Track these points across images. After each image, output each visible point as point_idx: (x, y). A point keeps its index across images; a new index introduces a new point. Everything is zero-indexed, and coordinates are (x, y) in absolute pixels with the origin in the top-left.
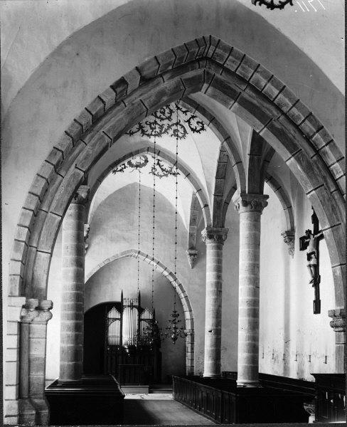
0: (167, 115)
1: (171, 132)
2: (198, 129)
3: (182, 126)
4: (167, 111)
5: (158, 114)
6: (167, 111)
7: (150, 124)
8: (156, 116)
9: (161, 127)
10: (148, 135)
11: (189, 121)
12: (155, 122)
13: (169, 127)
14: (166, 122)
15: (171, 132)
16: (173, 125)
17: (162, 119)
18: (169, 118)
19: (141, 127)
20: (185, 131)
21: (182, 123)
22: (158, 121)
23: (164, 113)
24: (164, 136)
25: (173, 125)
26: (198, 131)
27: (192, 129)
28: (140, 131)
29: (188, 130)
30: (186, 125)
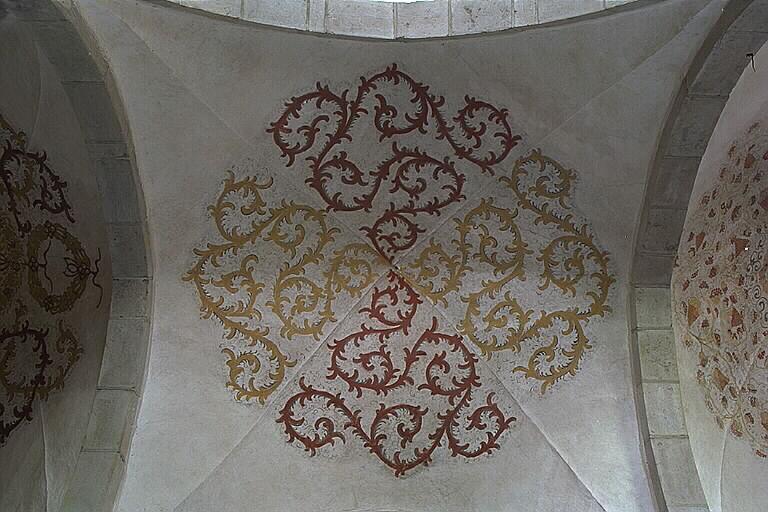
0: (298, 320)
1: (239, 346)
2: (299, 429)
3: (280, 377)
4: (312, 317)
5: (292, 293)
6: (312, 317)
7: (246, 274)
8: (278, 290)
9: (248, 312)
10: (195, 274)
11: (309, 392)
12: (254, 292)
13: (258, 336)
14: (271, 319)
15: (239, 346)
16: (270, 345)
17: (277, 309)
18: (289, 330)
19: (236, 241)
20: (263, 393)
21: (291, 374)
22: (261, 299)
23: (299, 308)
24: (217, 331)
25: (270, 345)
26: (294, 435)
27: (286, 416)
28: (219, 241)
29: (277, 399)
30: (288, 388)
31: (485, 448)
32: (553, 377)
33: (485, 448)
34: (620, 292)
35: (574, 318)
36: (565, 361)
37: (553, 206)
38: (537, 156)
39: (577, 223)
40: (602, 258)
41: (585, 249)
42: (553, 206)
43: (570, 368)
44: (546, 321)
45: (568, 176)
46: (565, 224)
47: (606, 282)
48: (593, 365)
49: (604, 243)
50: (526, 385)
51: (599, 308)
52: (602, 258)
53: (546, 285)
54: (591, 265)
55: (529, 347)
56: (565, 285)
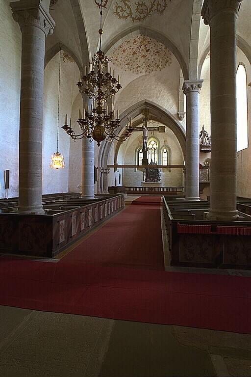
31: (98, 4)
32: (117, 13)
33: (98, 4)
34: (137, 23)
35: (131, 14)
36: (121, 15)
37: (155, 7)
38: (166, 5)
39: (151, 13)
40: (144, 18)
41: (145, 14)
42: (155, 7)
43: (120, 17)
44: (129, 7)
45: (161, 12)
46: (151, 10)
47: (139, 19)
48: (122, 22)
49: (147, 19)
50: (114, 7)
51: (133, 19)
52: (144, 18)
53: (136, 5)
54: (142, 16)
55: (121, 4)
56: (137, 9)
